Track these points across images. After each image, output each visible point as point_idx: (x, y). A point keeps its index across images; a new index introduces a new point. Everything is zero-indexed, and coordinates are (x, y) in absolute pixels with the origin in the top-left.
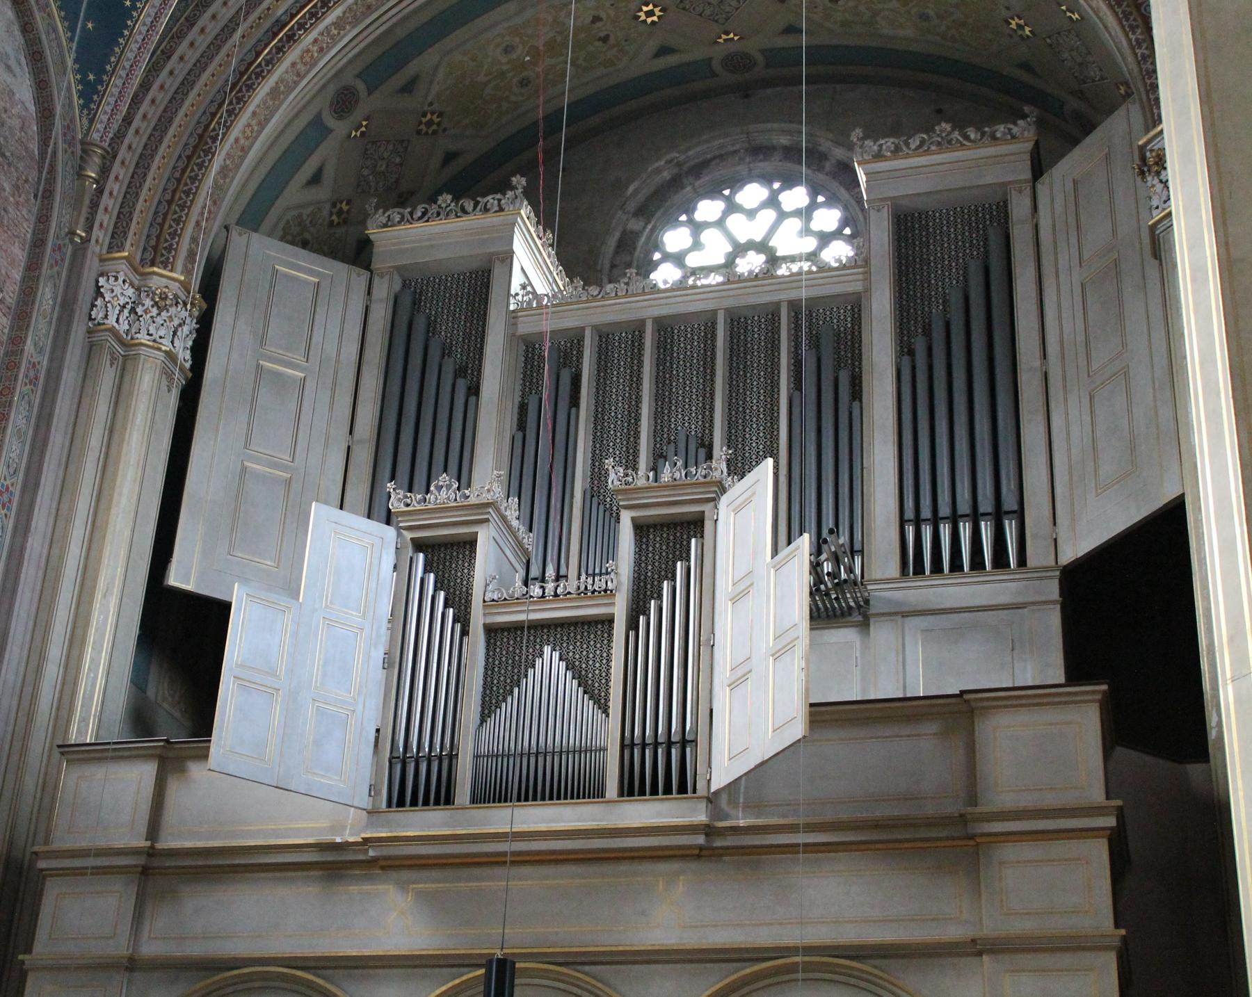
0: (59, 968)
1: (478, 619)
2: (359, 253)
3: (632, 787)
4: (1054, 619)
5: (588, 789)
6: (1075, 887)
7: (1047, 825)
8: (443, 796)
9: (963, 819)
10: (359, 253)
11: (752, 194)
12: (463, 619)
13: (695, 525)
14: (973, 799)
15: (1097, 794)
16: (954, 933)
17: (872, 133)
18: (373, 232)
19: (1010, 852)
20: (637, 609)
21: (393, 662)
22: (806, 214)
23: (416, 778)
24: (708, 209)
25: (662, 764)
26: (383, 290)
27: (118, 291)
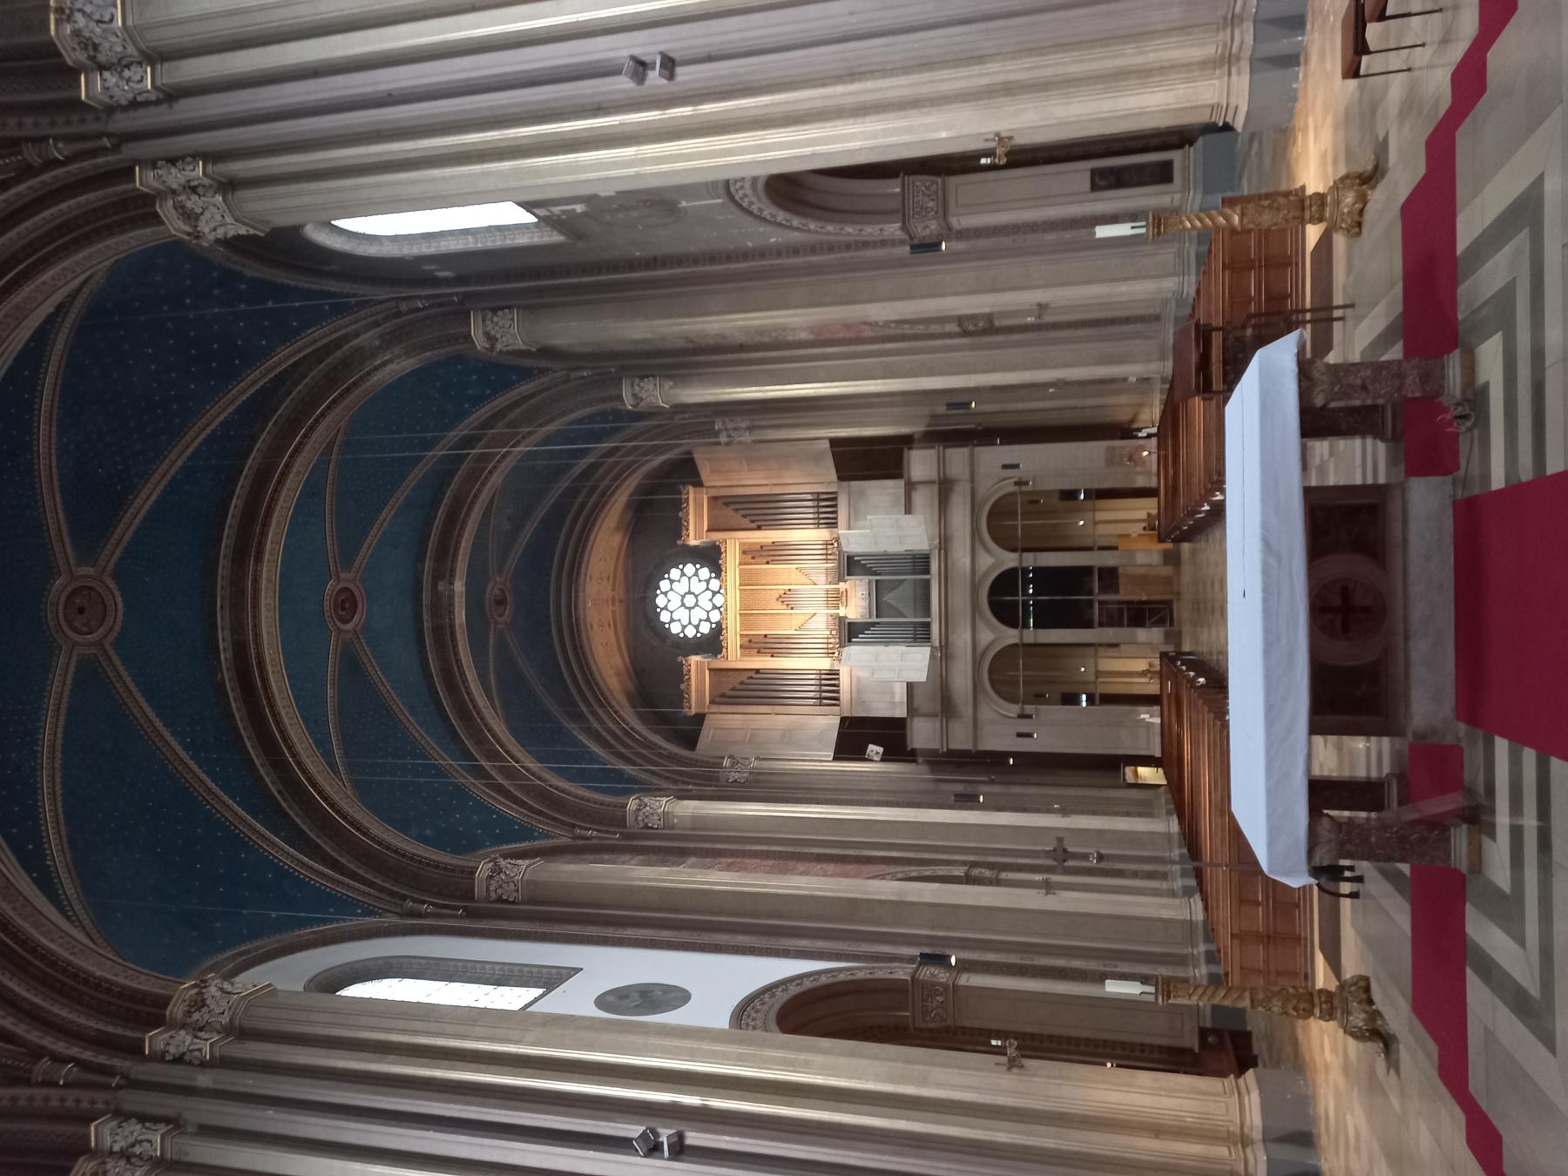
0: (976, 739)
1: (875, 619)
2: (700, 718)
3: (927, 571)
4: (853, 483)
5: (927, 584)
6: (958, 458)
7: (942, 463)
8: (927, 626)
9: (941, 483)
10: (700, 718)
11: (660, 601)
12: (874, 624)
13: (850, 558)
14: (932, 482)
15: (933, 452)
16: (968, 486)
17: (680, 537)
18: (693, 711)
19: (948, 472)
20: (875, 574)
21: (887, 644)
22: (672, 582)
23: (920, 634)
24: (665, 617)
25: (920, 562)
26: (714, 708)
27: (734, 776)
